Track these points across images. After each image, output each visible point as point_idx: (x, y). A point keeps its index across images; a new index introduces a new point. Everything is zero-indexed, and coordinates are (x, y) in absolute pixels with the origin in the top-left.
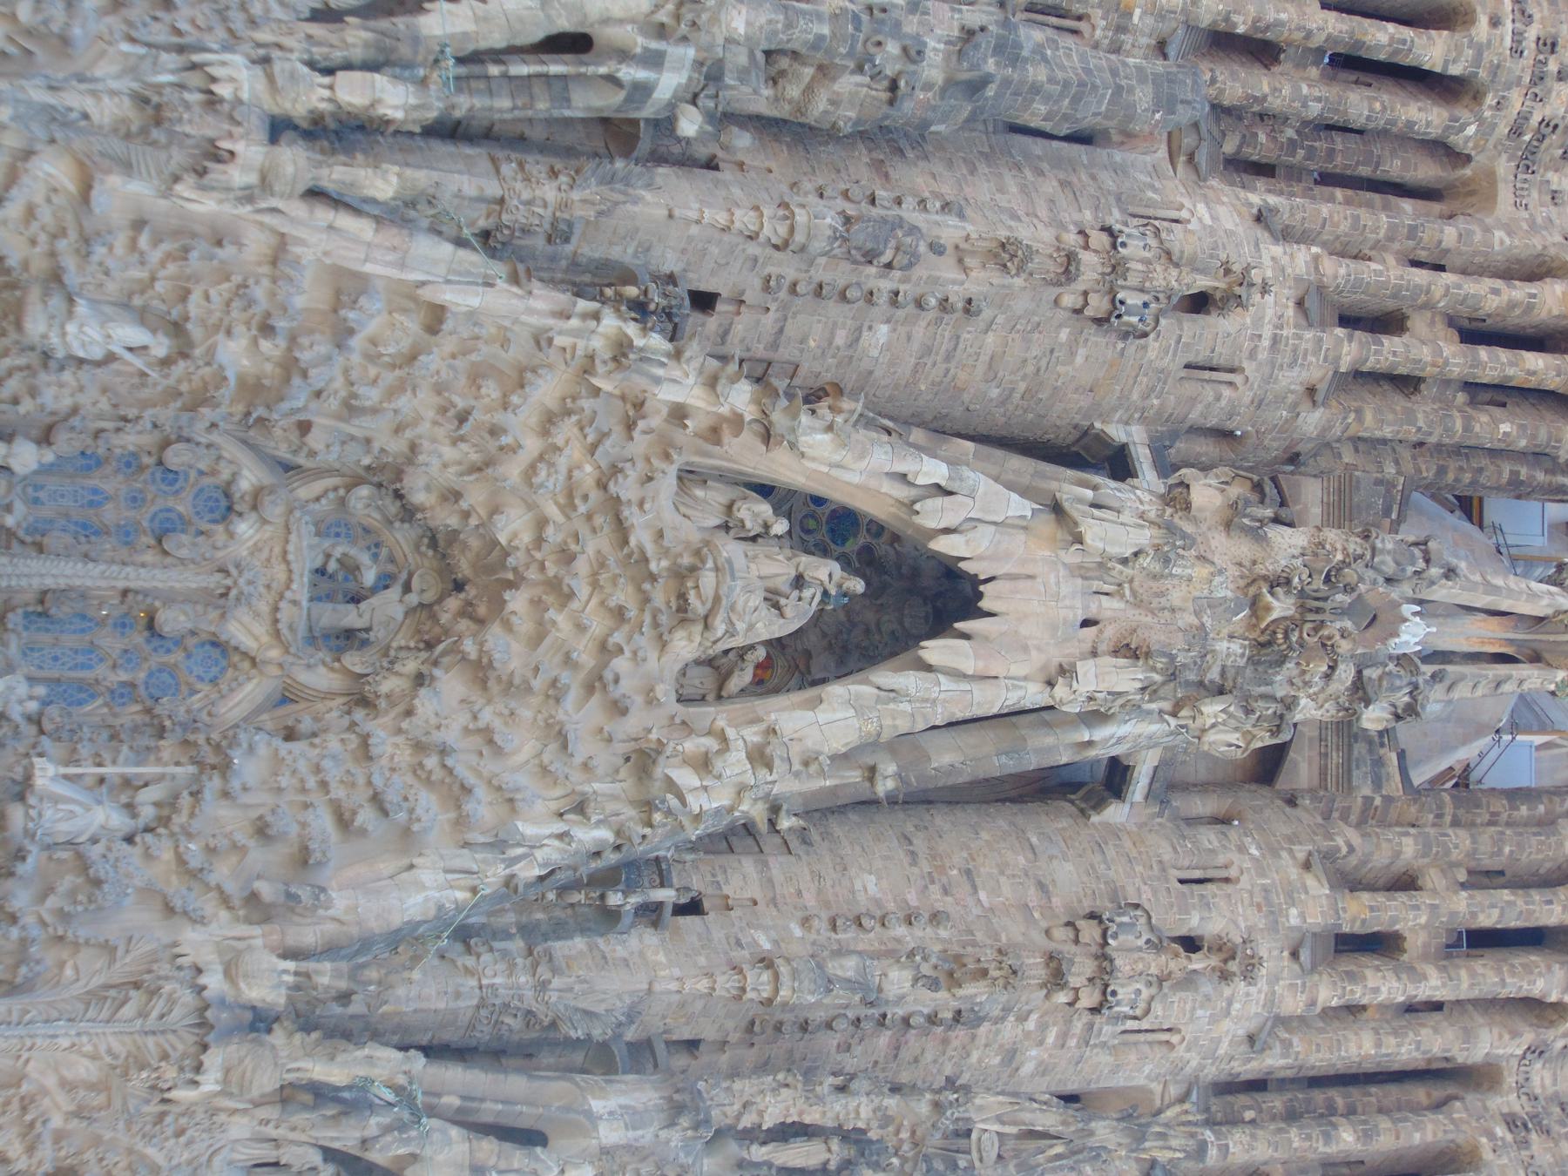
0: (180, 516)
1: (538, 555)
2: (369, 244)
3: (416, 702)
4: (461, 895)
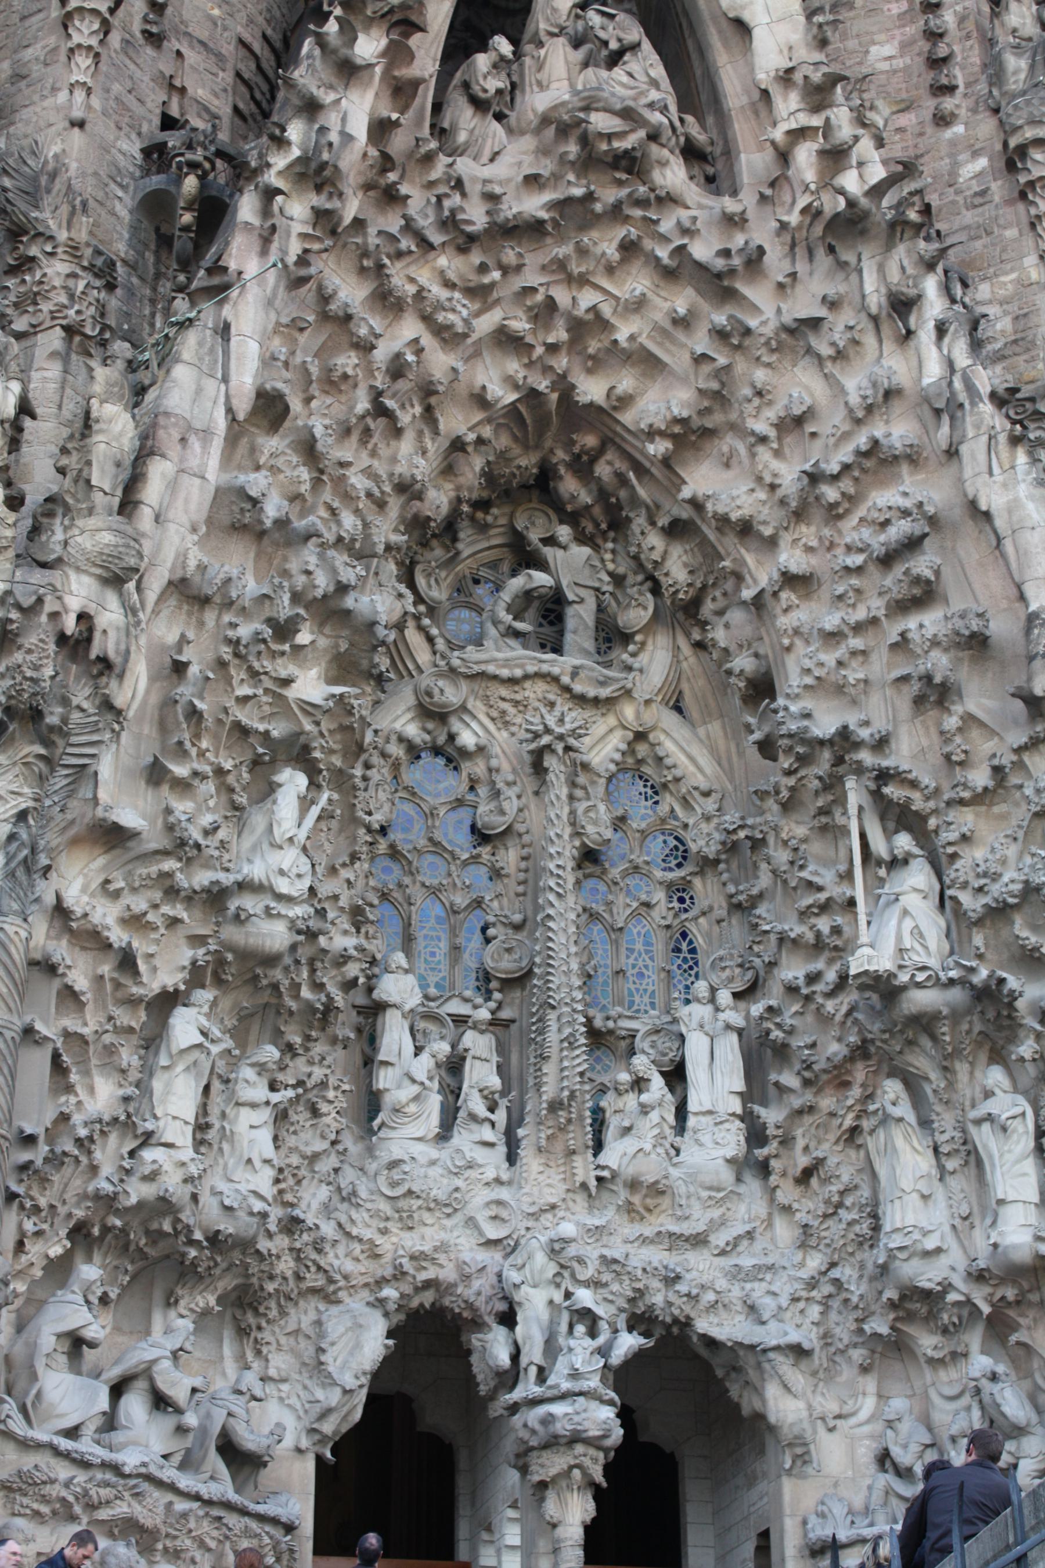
1: (539, 350)
4: (1021, 457)
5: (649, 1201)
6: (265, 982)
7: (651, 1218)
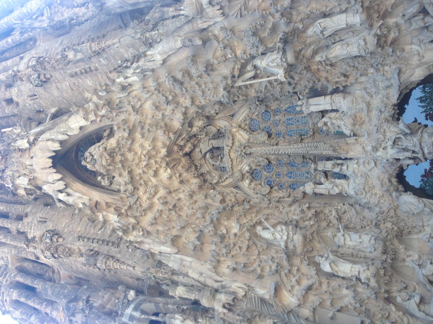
0: (265, 171)
1: (157, 166)
2: (191, 267)
3: (182, 118)
5: (358, 120)
6: (311, 237)
7: (364, 117)
